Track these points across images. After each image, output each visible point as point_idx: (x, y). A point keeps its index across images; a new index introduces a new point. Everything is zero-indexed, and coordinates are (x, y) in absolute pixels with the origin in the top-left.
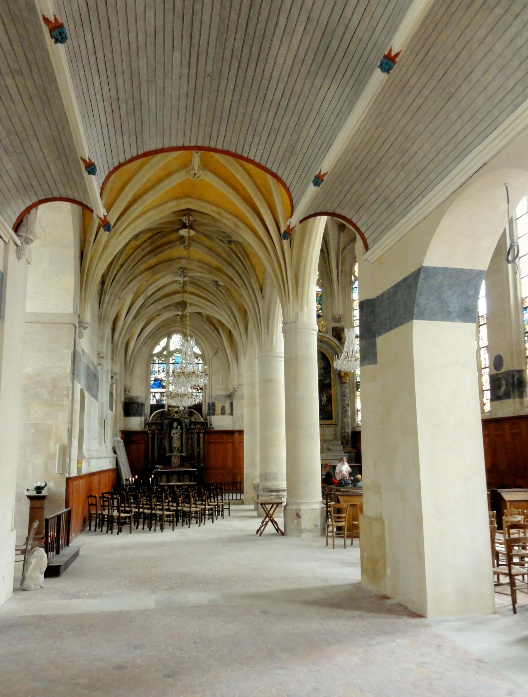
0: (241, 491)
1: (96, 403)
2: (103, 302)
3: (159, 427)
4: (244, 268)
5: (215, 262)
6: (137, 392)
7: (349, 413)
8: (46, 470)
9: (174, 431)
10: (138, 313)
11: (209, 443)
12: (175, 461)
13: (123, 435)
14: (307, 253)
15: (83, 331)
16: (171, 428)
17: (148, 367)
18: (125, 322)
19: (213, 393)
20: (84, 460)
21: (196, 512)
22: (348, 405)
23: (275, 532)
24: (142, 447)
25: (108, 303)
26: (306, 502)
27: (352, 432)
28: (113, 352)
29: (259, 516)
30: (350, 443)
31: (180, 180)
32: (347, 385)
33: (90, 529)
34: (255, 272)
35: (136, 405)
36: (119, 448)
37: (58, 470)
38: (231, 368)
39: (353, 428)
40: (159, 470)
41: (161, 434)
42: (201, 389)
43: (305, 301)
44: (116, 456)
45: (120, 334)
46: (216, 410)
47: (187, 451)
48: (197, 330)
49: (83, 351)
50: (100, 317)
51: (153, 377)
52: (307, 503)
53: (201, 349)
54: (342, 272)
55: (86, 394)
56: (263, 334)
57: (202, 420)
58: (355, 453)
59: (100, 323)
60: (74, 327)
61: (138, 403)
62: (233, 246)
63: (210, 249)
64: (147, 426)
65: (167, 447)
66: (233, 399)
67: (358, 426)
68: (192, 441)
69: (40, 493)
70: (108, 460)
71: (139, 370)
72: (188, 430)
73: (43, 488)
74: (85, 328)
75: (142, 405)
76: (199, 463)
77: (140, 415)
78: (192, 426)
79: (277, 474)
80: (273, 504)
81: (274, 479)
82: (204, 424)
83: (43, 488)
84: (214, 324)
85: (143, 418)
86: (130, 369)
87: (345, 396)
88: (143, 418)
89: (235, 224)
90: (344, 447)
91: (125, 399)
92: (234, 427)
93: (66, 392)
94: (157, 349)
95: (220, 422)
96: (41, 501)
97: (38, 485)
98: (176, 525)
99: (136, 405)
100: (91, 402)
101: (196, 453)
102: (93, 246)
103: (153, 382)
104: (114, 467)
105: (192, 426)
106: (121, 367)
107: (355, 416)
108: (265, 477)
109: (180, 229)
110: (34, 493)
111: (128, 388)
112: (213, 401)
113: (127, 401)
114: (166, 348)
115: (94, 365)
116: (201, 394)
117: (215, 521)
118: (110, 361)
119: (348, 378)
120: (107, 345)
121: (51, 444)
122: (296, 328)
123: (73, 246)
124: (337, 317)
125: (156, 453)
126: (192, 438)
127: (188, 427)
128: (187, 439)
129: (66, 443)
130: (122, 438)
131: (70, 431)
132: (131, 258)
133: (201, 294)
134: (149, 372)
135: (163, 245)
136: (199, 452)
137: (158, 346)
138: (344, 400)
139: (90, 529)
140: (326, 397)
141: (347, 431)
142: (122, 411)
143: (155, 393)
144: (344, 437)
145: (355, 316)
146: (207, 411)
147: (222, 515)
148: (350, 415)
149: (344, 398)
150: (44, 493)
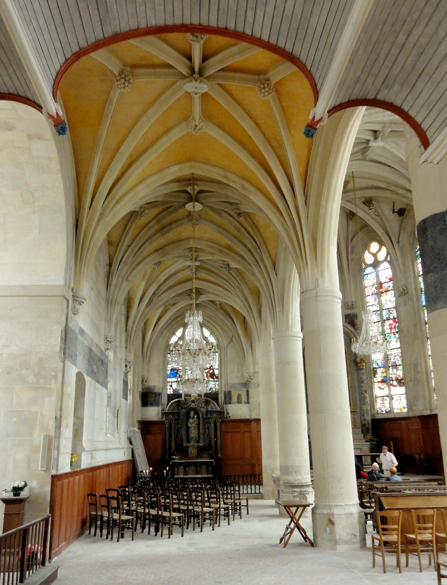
0: (260, 483)
1: (104, 390)
2: (111, 285)
3: (176, 417)
4: (255, 244)
5: (225, 241)
6: (154, 382)
7: (368, 400)
8: (29, 466)
9: (191, 421)
10: (151, 301)
11: (226, 432)
12: (192, 451)
13: (141, 425)
14: (326, 208)
15: (78, 306)
16: (188, 417)
17: (165, 356)
18: (138, 311)
20: (83, 453)
21: (211, 513)
22: (366, 391)
23: (303, 541)
24: (160, 437)
25: (116, 286)
26: (340, 504)
27: (372, 420)
28: (127, 341)
29: (281, 516)
30: (370, 431)
31: (180, 135)
32: (363, 371)
33: (90, 533)
34: (267, 247)
35: (154, 395)
36: (135, 439)
37: (42, 467)
38: (246, 356)
39: (373, 415)
40: (176, 461)
41: (178, 424)
42: (217, 378)
43: (326, 265)
44: (132, 447)
45: (134, 322)
46: (233, 399)
47: (204, 441)
48: (211, 319)
49: (82, 332)
50: (107, 300)
51: (169, 367)
52: (341, 506)
53: (217, 338)
54: (352, 260)
55: (88, 379)
56: (278, 313)
57: (219, 409)
58: (377, 441)
59: (108, 307)
60: (65, 302)
61: (156, 393)
62: (242, 219)
63: (219, 226)
64: (164, 416)
65: (184, 437)
66: (249, 387)
67: (378, 413)
68: (209, 431)
69: (18, 495)
70: (122, 452)
71: (156, 360)
72: (204, 419)
73: (21, 489)
74: (80, 303)
75: (160, 394)
76: (216, 453)
77: (157, 405)
78: (209, 416)
79: (299, 466)
80: (298, 507)
81: (295, 472)
82: (221, 413)
83: (21, 489)
84: (229, 313)
85: (160, 408)
86: (147, 359)
87: (362, 382)
88: (160, 408)
89: (243, 187)
90: (364, 436)
91: (143, 389)
92: (250, 416)
93: (54, 374)
94: (174, 339)
95: (237, 411)
96: (17, 506)
97: (16, 485)
98: (187, 528)
99: (154, 395)
100: (95, 388)
101: (213, 443)
102: (88, 213)
103: (170, 371)
104: (130, 458)
105: (209, 416)
106: (135, 355)
107: (373, 402)
108: (286, 469)
109: (187, 203)
110: (10, 495)
111: (145, 378)
113: (145, 391)
114: (182, 338)
115: (100, 349)
116: (217, 383)
117: (231, 522)
118: (123, 350)
119: (364, 364)
120: (121, 334)
121: (36, 434)
122: (317, 296)
123: (64, 211)
124: (350, 304)
125: (173, 444)
126: (208, 428)
127: (205, 417)
128: (205, 429)
129: (52, 433)
130: (139, 429)
131: (59, 421)
132: (138, 238)
133: (213, 279)
134: (165, 363)
135: (170, 224)
136: (216, 442)
137: (175, 336)
139: (90, 533)
141: (367, 418)
142: (140, 401)
143: (172, 382)
144: (364, 425)
145: (368, 302)
146: (223, 400)
147: (240, 514)
150: (24, 494)
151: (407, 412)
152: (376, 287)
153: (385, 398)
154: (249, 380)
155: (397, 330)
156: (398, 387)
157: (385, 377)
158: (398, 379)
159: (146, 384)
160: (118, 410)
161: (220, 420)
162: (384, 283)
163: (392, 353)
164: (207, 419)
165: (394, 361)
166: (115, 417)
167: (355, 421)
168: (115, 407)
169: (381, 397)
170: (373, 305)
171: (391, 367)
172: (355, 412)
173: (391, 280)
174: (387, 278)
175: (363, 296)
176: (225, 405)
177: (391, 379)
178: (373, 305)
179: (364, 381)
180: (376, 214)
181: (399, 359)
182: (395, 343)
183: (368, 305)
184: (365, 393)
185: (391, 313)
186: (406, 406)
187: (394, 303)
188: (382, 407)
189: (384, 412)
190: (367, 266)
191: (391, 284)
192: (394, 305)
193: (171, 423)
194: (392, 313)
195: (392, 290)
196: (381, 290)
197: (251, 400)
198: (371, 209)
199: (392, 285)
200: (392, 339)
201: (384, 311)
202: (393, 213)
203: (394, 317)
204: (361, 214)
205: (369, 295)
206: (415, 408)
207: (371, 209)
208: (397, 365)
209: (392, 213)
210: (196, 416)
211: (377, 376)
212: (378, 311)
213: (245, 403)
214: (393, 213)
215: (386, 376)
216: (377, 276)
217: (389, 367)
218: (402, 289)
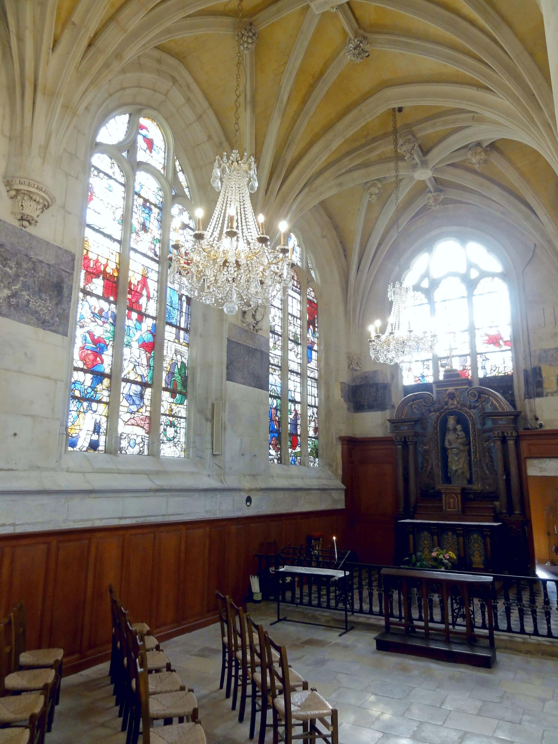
9: (450, 436)
12: (452, 503)
13: (346, 446)
16: (444, 430)
19: (532, 349)
46: (545, 385)
61: (377, 385)
65: (438, 472)
78: (489, 424)
91: (354, 380)
105: (489, 424)
112: (535, 363)
142: (342, 400)
159: (358, 368)
160: (213, 405)
161: (514, 434)
164: (485, 432)
166: (207, 420)
168: (207, 398)
176: (527, 400)
193: (405, 440)
210: (459, 427)
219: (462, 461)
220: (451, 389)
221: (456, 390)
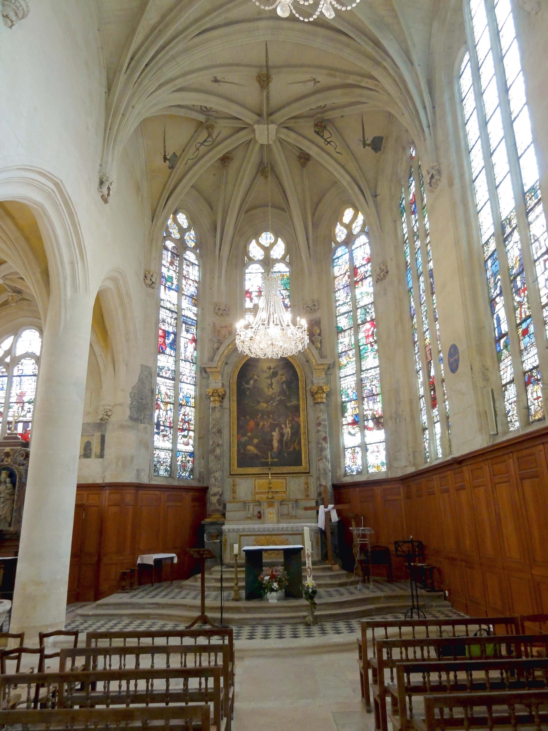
7: (328, 453)
22: (325, 439)
32: (322, 406)
67: (345, 475)
87: (319, 424)
107: (339, 458)
138: (318, 431)
140: (292, 428)
141: (324, 483)
148: (329, 457)
149: (320, 428)
151: (386, 472)
152: (349, 276)
153: (358, 449)
154: (105, 417)
155: (375, 338)
156: (375, 431)
157: (357, 415)
158: (376, 418)
162: (359, 268)
163: (368, 375)
165: (370, 388)
167: (308, 487)
169: (351, 448)
170: (344, 303)
171: (366, 399)
172: (309, 473)
173: (369, 260)
174: (363, 258)
175: (331, 291)
177: (365, 418)
178: (344, 303)
179: (323, 423)
180: (338, 150)
181: (377, 385)
182: (371, 361)
183: (337, 304)
184: (324, 442)
185: (368, 312)
186: (385, 461)
187: (372, 296)
188: (352, 463)
189: (355, 473)
190: (339, 245)
191: (369, 267)
192: (370, 299)
194: (370, 312)
195: (370, 276)
196: (355, 279)
197: (106, 451)
198: (329, 143)
199: (370, 269)
200: (368, 354)
201: (359, 310)
202: (364, 147)
203: (371, 318)
204: (313, 151)
205: (339, 290)
206: (396, 464)
207: (329, 143)
208: (374, 395)
209: (363, 146)
211: (346, 415)
212: (351, 311)
213: (97, 457)
214: (364, 147)
215: (358, 414)
216: (351, 259)
217: (363, 398)
218: (379, 270)
219: (7, 507)
220: (7, 449)
221: (12, 450)
